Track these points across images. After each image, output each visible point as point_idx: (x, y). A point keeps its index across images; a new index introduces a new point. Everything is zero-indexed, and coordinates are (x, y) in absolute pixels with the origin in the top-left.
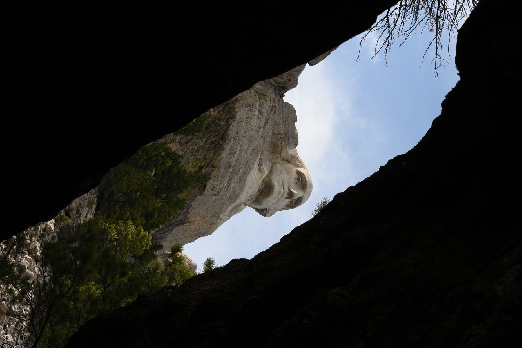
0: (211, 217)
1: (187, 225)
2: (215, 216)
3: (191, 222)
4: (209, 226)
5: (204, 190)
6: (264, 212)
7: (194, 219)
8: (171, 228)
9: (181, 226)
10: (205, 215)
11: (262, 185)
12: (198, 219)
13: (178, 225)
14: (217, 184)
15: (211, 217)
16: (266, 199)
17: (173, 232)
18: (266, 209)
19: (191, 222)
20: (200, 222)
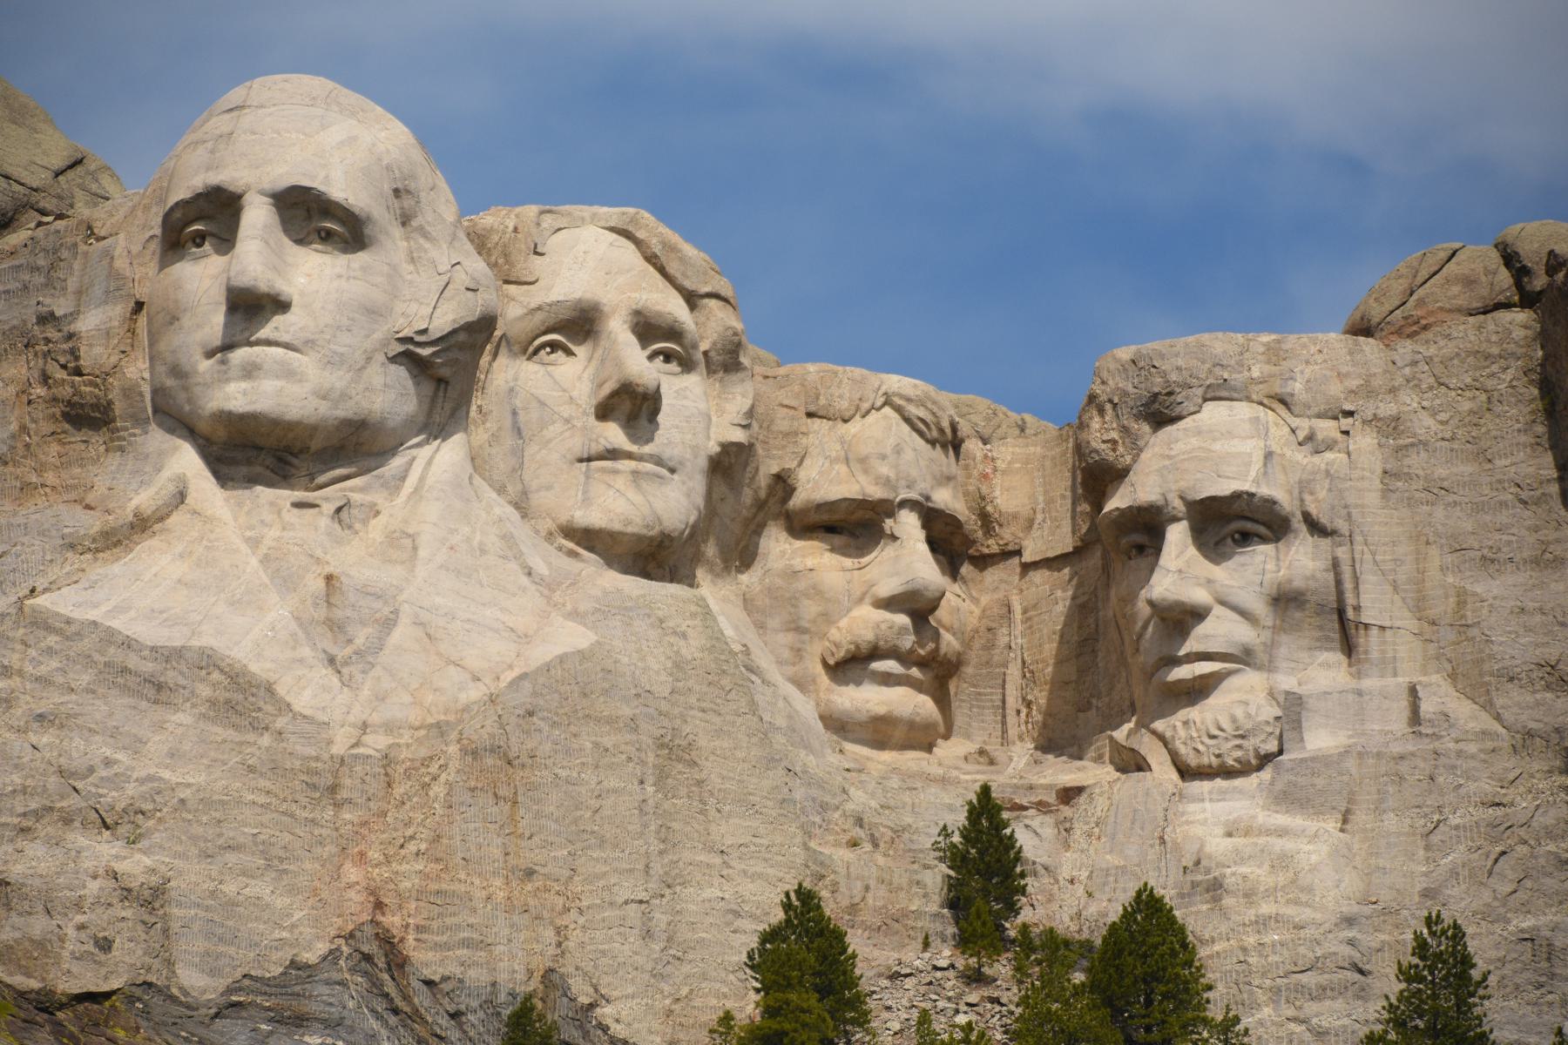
0: (338, 805)
1: (392, 921)
2: (333, 789)
3: (379, 905)
4: (399, 791)
5: (108, 995)
6: (425, 352)
7: (356, 897)
8: (422, 999)
9: (410, 947)
10: (330, 849)
11: (249, 462)
12: (352, 873)
13: (398, 963)
14: (81, 927)
15: (338, 805)
16: (313, 420)
17: (453, 969)
18: (393, 360)
19: (379, 905)
20: (374, 855)
